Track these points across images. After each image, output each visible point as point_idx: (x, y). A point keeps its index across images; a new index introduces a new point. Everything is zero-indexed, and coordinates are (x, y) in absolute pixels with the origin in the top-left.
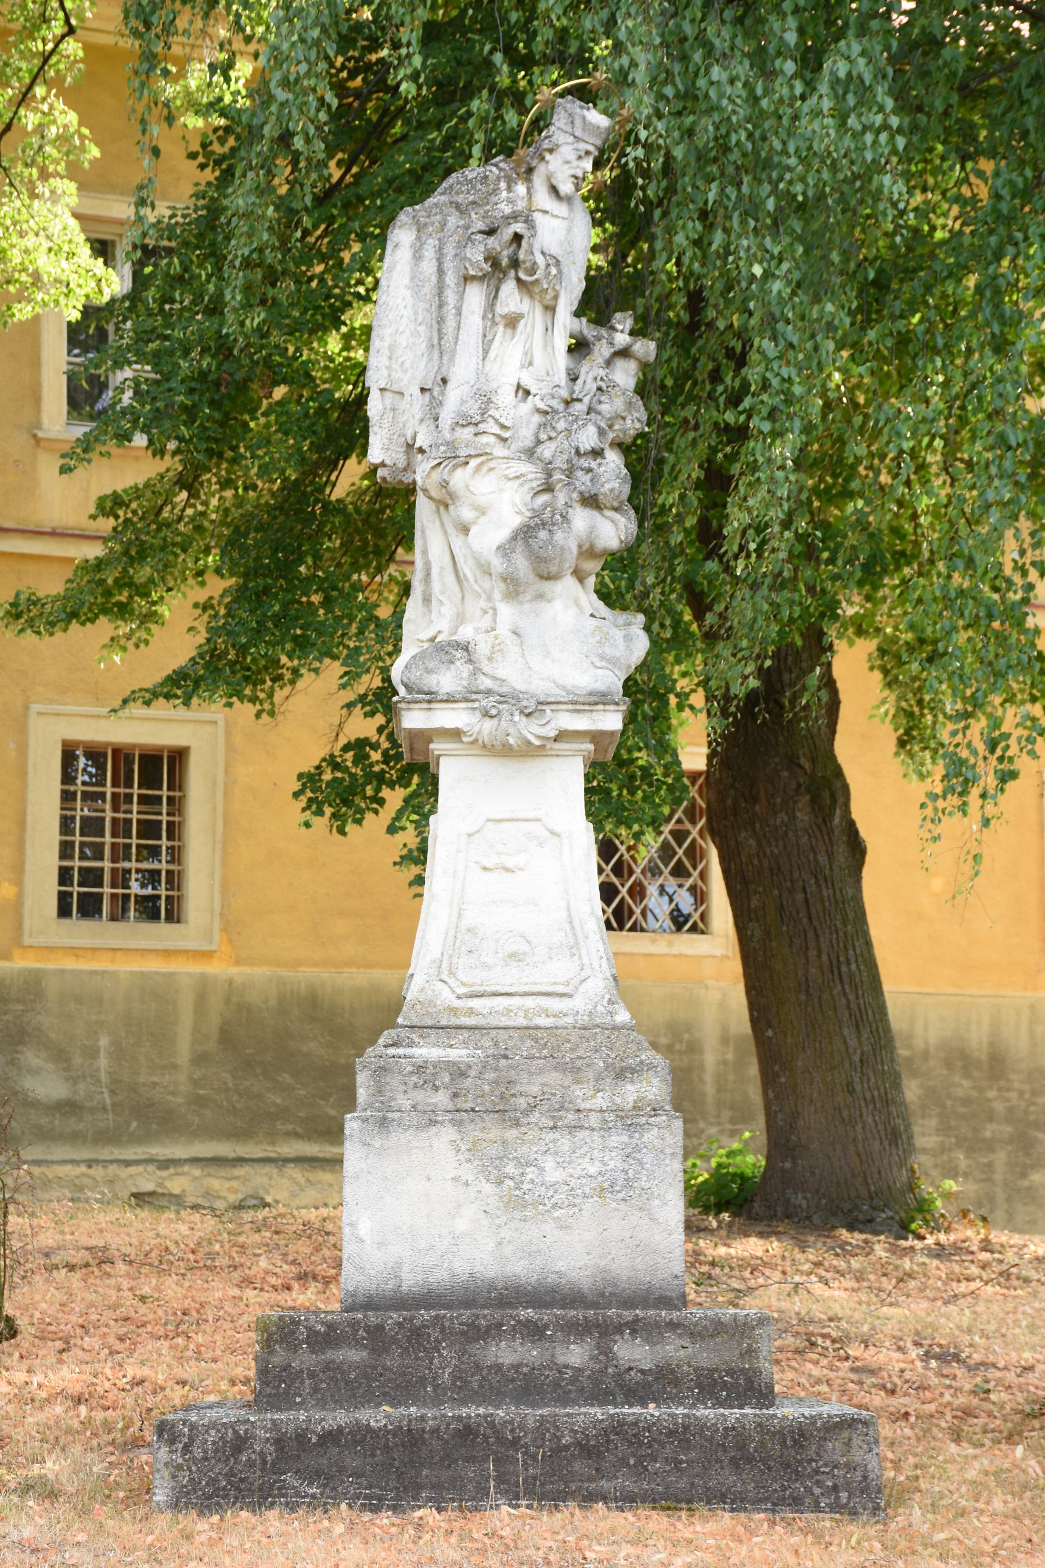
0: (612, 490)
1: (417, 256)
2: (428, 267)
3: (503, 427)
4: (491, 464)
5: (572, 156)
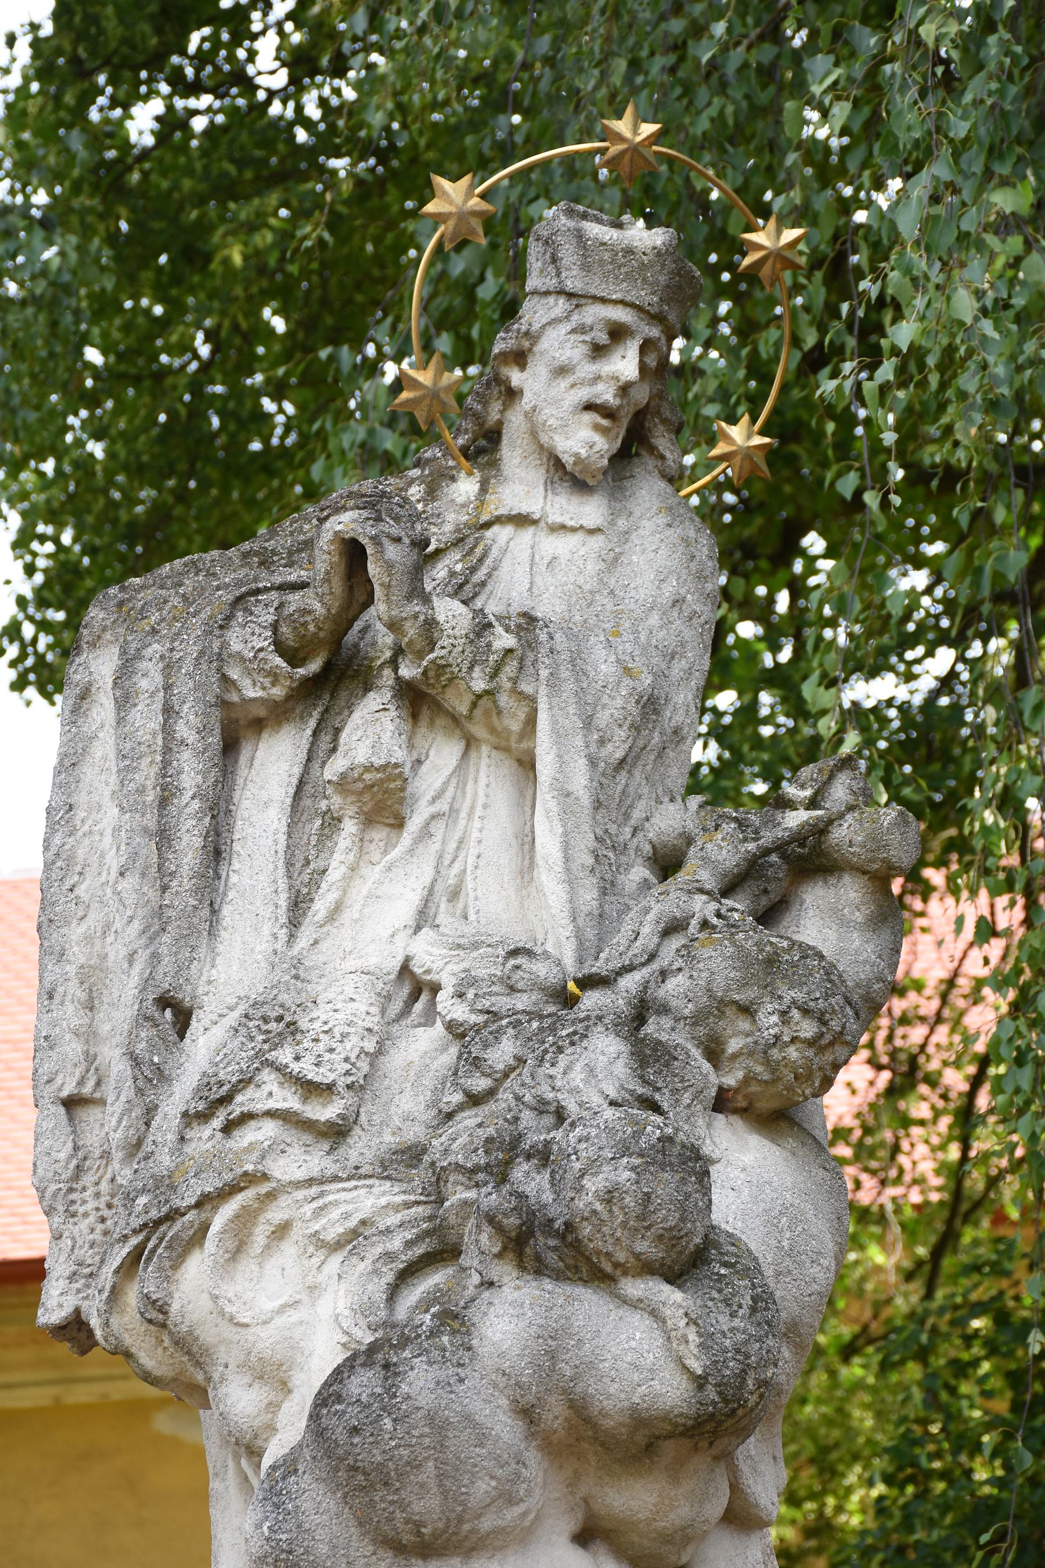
0: (610, 1196)
1: (124, 701)
2: (146, 719)
3: (310, 1089)
4: (276, 1214)
5: (573, 351)
